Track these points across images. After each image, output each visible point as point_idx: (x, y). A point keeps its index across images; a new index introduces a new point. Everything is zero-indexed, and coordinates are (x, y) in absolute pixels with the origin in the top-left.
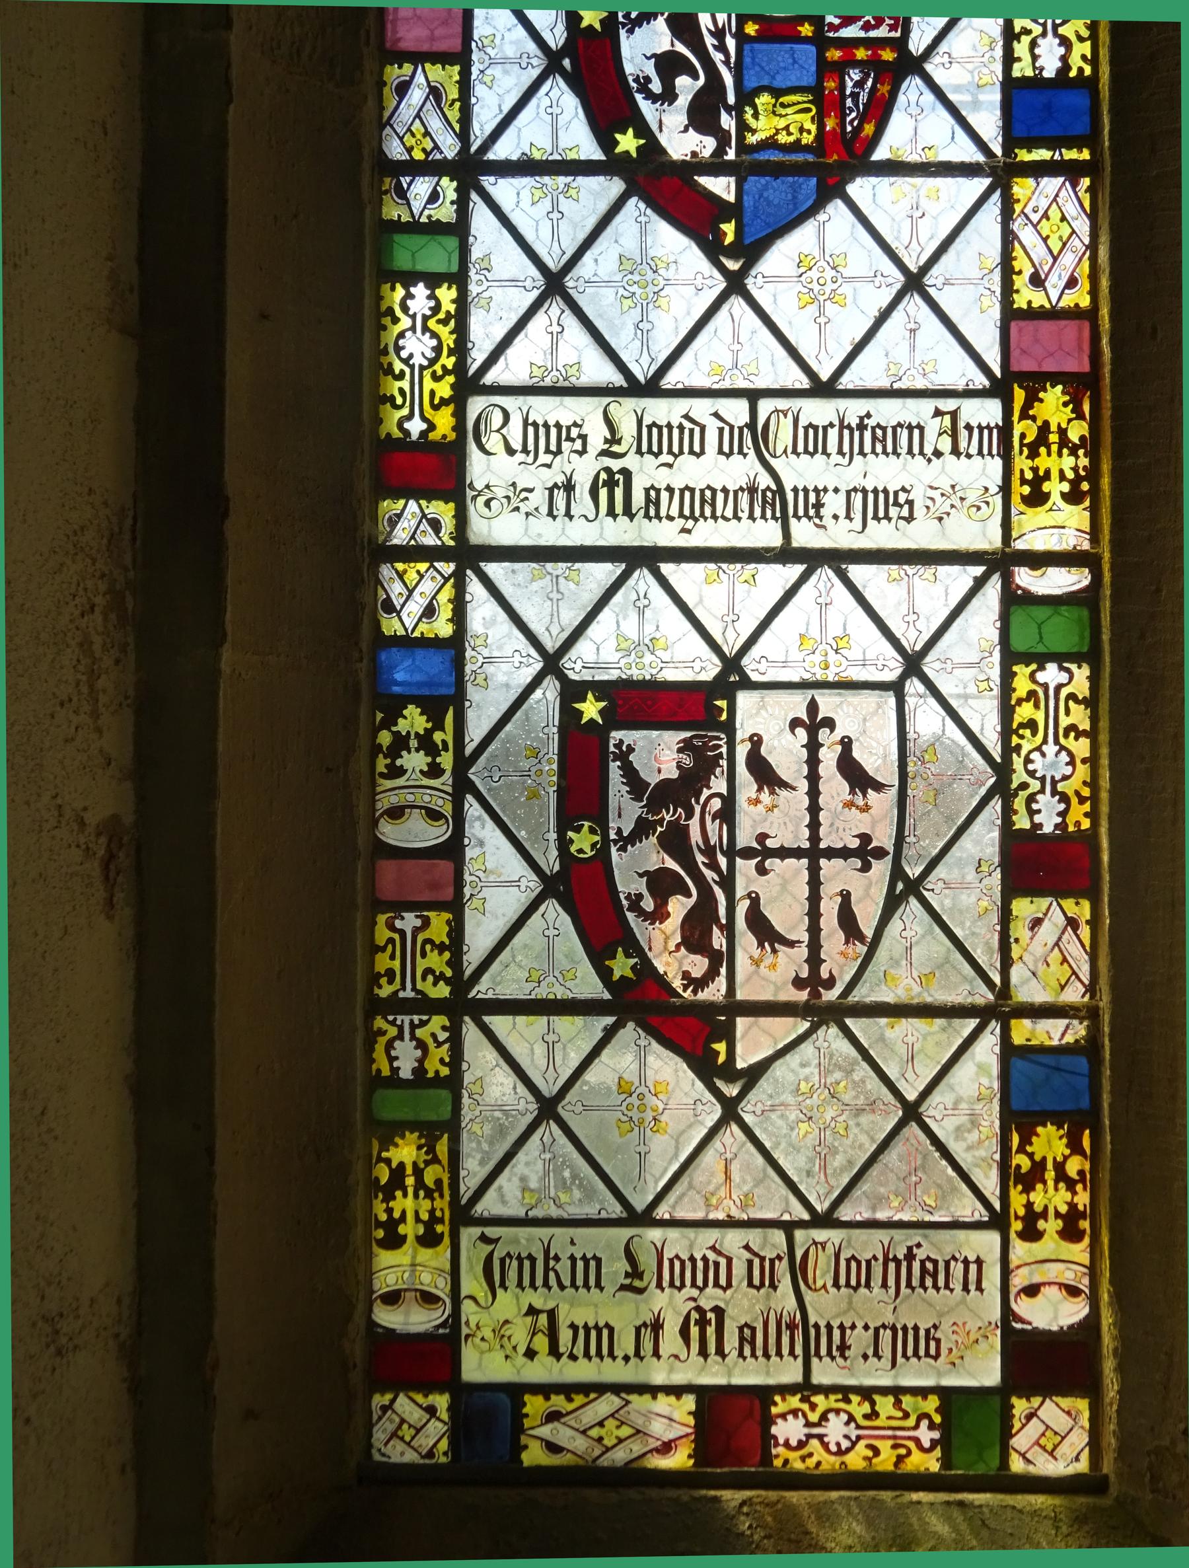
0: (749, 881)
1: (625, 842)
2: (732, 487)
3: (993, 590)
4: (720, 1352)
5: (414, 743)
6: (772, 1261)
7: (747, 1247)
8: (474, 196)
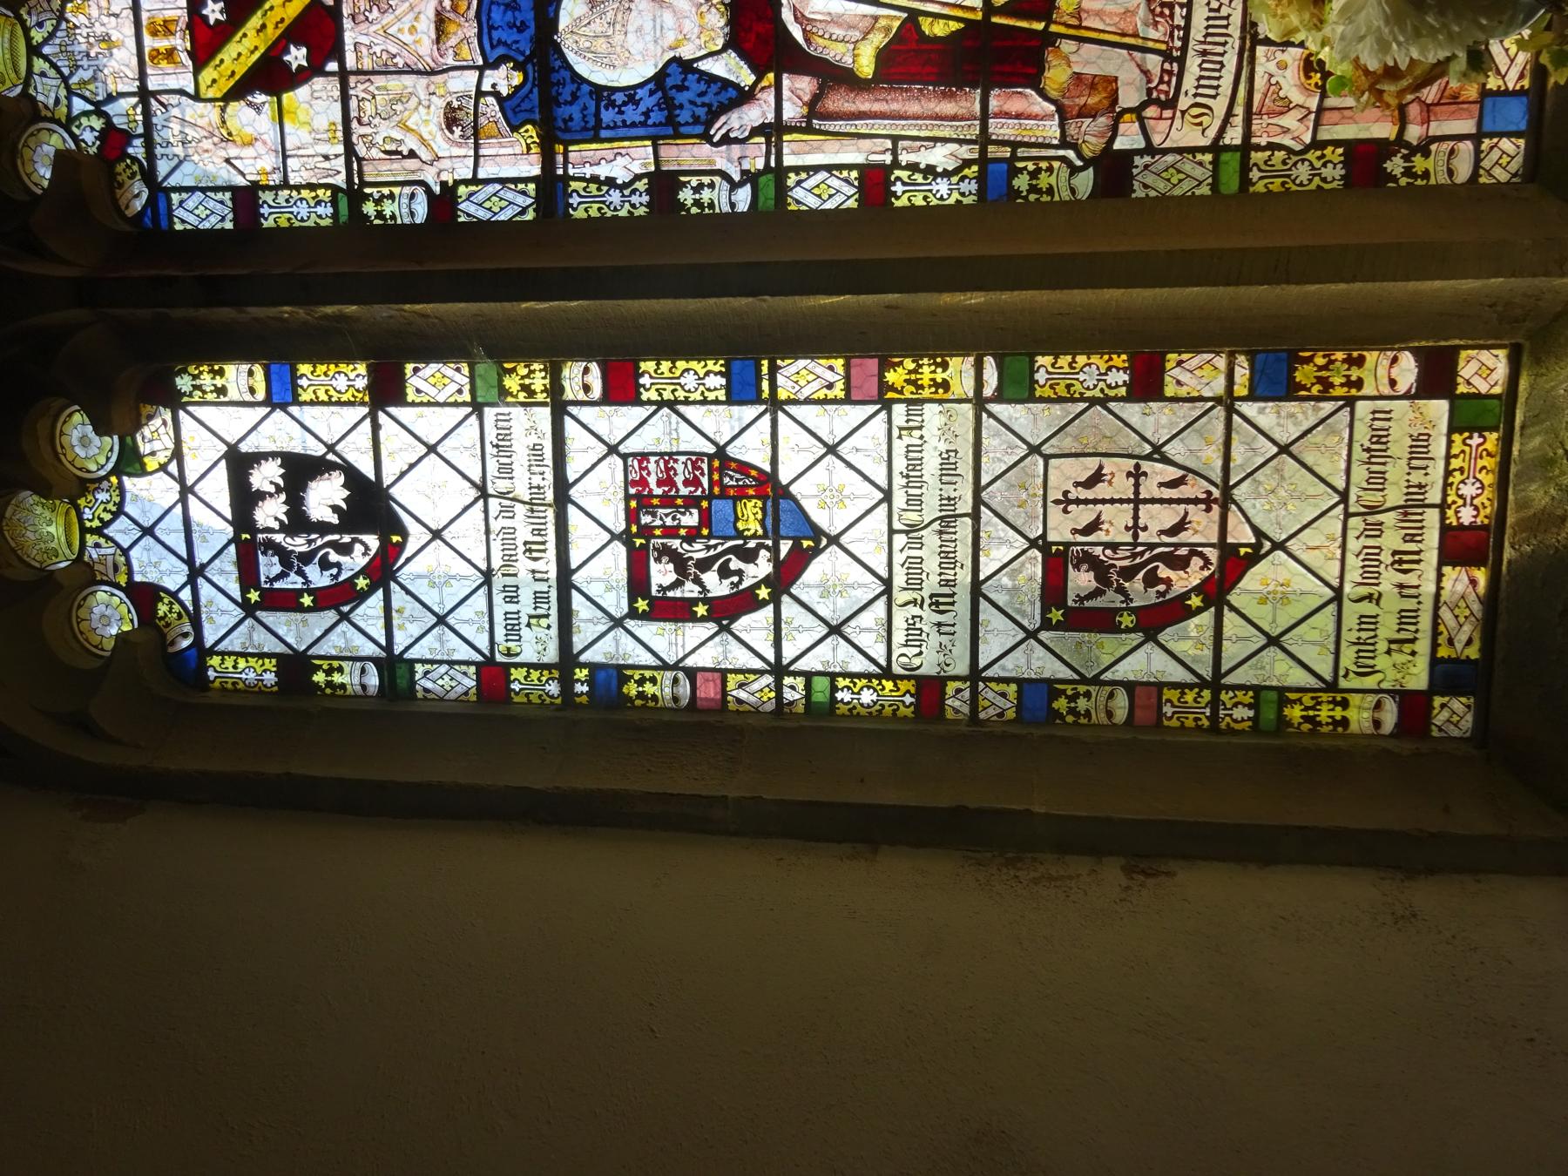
0: (1151, 536)
1: (1128, 599)
2: (939, 543)
3: (995, 408)
4: (1418, 553)
5: (1073, 705)
6: (1367, 524)
7: (1358, 538)
8: (792, 668)
